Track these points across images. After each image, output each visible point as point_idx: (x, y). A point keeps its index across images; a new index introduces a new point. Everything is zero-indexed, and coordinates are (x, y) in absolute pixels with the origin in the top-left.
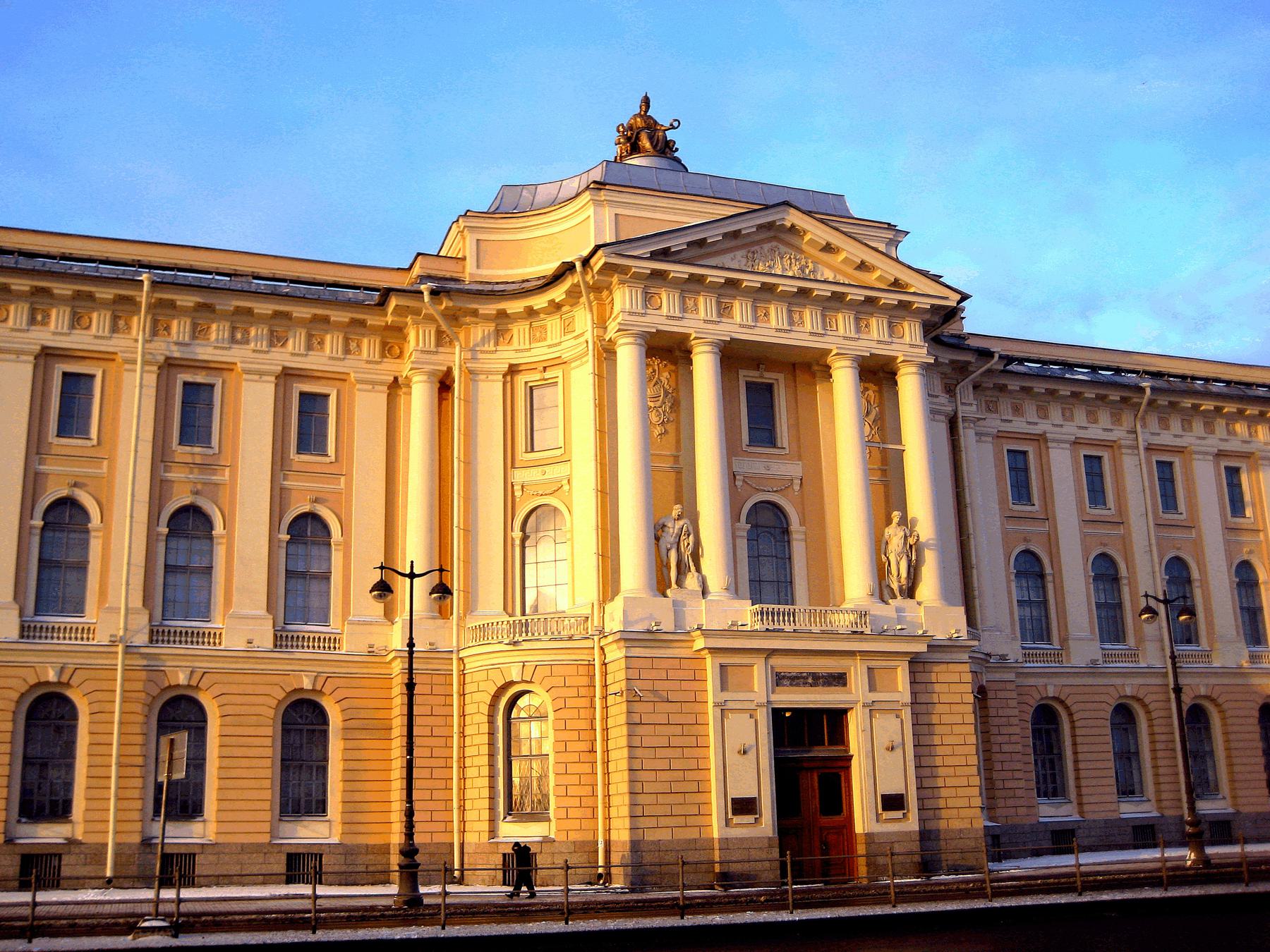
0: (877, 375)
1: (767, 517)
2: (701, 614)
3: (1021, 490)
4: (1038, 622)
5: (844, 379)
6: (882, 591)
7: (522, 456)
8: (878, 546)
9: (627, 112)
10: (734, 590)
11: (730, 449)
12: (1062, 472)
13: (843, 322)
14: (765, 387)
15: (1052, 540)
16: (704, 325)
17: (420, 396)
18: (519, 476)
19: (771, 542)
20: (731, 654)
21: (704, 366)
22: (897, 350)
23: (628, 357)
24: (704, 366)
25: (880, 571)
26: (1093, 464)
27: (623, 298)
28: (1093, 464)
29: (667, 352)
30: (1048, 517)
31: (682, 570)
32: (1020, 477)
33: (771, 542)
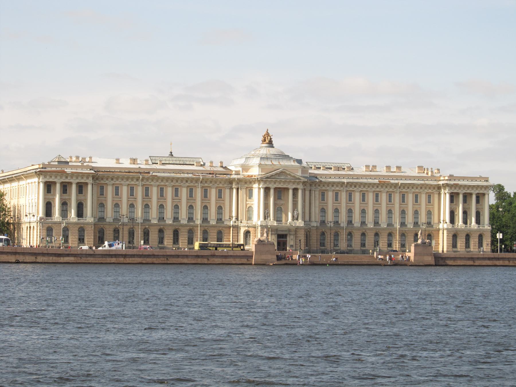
0: (295, 190)
1: (279, 209)
2: (270, 224)
5: (291, 192)
7: (248, 200)
9: (264, 133)
10: (274, 220)
11: (275, 200)
13: (291, 184)
14: (280, 192)
15: (327, 206)
17: (235, 191)
18: (247, 202)
21: (272, 192)
22: (298, 187)
24: (272, 192)
25: (293, 217)
29: (267, 190)
31: (268, 217)
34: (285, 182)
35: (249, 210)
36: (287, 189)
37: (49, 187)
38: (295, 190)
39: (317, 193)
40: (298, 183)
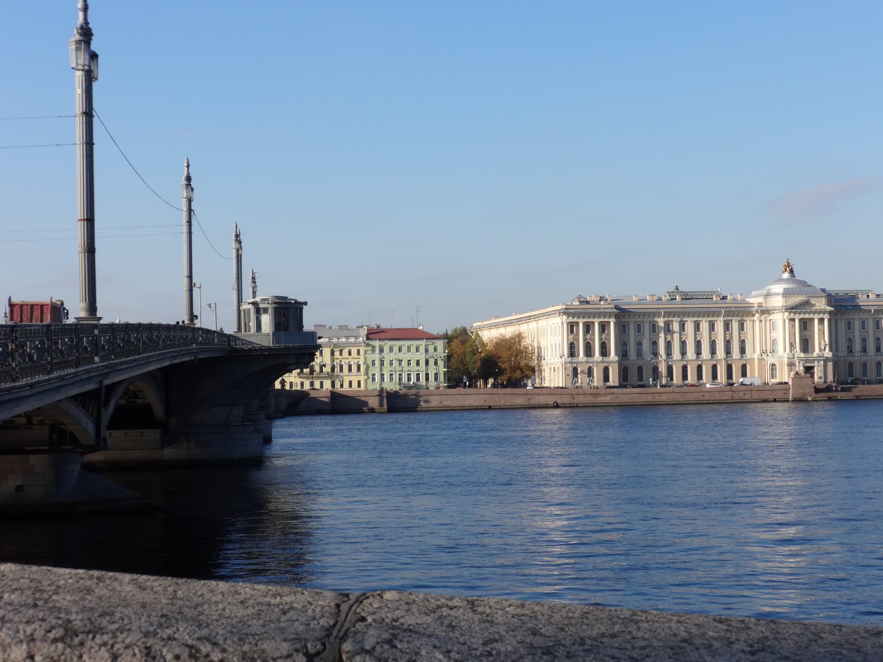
0: (821, 321)
3: (849, 328)
4: (850, 350)
5: (816, 321)
6: (821, 350)
8: (820, 344)
12: (857, 325)
15: (854, 336)
16: (797, 317)
19: (806, 345)
20: (800, 359)
23: (787, 321)
24: (797, 322)
26: (863, 322)
27: (786, 314)
28: (863, 322)
30: (854, 332)
32: (849, 325)
33: (806, 345)
34: (810, 313)
35: (774, 342)
36: (813, 319)
37: (572, 327)
38: (821, 321)
39: (843, 322)
40: (824, 313)
